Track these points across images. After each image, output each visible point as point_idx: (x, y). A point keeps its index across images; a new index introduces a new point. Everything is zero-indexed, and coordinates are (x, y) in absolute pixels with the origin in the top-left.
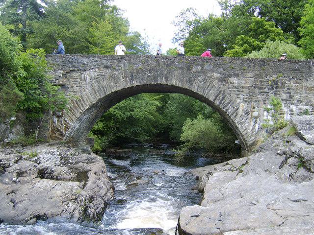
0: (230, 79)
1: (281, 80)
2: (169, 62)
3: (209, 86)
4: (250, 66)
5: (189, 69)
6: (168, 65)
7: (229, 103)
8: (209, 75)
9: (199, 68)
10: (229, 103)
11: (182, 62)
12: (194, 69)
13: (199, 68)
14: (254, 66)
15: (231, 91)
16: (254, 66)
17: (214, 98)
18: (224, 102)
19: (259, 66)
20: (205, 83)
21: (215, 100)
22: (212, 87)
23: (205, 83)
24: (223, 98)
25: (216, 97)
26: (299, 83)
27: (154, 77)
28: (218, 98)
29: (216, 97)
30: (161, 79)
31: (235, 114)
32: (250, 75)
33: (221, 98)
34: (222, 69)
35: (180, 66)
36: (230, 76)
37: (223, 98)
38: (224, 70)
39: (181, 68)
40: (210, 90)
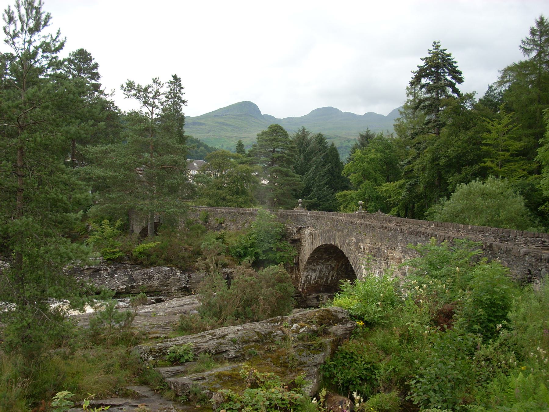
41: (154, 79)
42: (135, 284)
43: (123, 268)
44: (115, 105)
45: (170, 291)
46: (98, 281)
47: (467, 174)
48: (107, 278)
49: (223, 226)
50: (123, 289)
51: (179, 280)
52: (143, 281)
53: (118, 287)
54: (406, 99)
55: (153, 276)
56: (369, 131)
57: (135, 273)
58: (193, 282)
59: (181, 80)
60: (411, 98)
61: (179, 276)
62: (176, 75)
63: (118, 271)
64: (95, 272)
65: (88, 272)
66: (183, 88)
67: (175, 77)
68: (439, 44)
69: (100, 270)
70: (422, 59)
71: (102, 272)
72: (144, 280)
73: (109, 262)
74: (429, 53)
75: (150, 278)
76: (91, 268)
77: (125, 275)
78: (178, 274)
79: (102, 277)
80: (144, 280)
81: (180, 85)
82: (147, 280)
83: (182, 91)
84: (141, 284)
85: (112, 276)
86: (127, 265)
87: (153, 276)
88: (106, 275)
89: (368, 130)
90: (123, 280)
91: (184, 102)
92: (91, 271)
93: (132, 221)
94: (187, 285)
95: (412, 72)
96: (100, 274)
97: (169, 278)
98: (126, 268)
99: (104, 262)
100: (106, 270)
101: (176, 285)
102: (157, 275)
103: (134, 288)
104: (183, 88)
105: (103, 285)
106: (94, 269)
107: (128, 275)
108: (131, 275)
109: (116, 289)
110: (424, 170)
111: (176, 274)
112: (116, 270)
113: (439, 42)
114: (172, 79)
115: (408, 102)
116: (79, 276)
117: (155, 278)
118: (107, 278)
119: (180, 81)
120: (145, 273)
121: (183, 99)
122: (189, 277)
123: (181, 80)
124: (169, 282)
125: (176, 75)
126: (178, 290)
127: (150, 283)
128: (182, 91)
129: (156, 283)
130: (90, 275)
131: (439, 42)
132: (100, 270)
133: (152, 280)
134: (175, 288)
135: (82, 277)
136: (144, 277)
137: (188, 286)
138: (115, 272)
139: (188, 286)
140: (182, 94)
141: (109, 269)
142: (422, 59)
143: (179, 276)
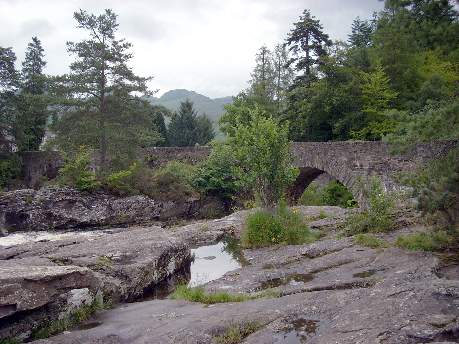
0: (354, 162)
1: (393, 162)
2: (313, 148)
3: (339, 168)
4: (367, 149)
5: (326, 153)
6: (312, 151)
7: (353, 185)
8: (339, 159)
9: (333, 152)
10: (353, 185)
11: (321, 148)
12: (329, 154)
13: (333, 152)
14: (371, 149)
15: (354, 173)
16: (371, 149)
17: (343, 179)
18: (350, 184)
19: (374, 148)
20: (337, 166)
21: (343, 181)
22: (342, 170)
23: (337, 166)
24: (349, 180)
25: (344, 179)
26: (407, 164)
27: (304, 162)
28: (345, 180)
29: (344, 179)
30: (308, 163)
31: (357, 195)
32: (369, 157)
33: (348, 180)
34: (347, 153)
35: (320, 151)
36: (353, 159)
37: (349, 180)
38: (349, 153)
39: (321, 153)
40: (340, 172)
41: (107, 10)
42: (114, 215)
43: (100, 199)
44: (13, 51)
45: (144, 221)
46: (76, 212)
47: (351, 119)
48: (84, 210)
49: (154, 164)
50: (102, 220)
51: (153, 209)
52: (122, 211)
53: (99, 218)
54: (256, 64)
55: (131, 206)
56: (189, 99)
57: (114, 203)
58: (164, 212)
59: (41, 43)
60: (260, 63)
61: (153, 205)
62: (36, 37)
63: (95, 202)
64: (70, 203)
65: (62, 204)
66: (43, 50)
67: (35, 40)
68: (309, 12)
69: (75, 201)
70: (294, 24)
71: (77, 203)
72: (123, 210)
73: (85, 192)
74: (301, 19)
75: (129, 207)
76: (66, 200)
77: (103, 205)
78: (153, 203)
79: (78, 208)
80: (123, 210)
81: (40, 48)
82: (125, 210)
83: (42, 52)
84: (119, 214)
85: (89, 208)
86: (105, 195)
87: (131, 206)
88: (82, 207)
89: (188, 98)
90: (102, 211)
91: (44, 63)
92: (66, 202)
93: (28, 168)
94: (158, 214)
95: (287, 34)
96: (75, 206)
97: (144, 208)
98: (103, 198)
99: (78, 193)
100: (81, 201)
101: (149, 215)
102: (134, 205)
103: (113, 219)
104: (43, 50)
105: (83, 216)
106: (70, 200)
107: (106, 205)
108: (109, 205)
109: (97, 220)
110: (304, 117)
111: (151, 204)
112: (93, 200)
113: (309, 10)
114: (32, 42)
115: (258, 67)
116: (54, 208)
117: (132, 208)
118: (84, 210)
119: (40, 44)
120: (123, 203)
121: (43, 61)
122: (162, 206)
123: (41, 43)
124: (144, 211)
125: (36, 37)
126: (150, 220)
127: (128, 214)
128: (42, 52)
129: (133, 212)
130: (65, 207)
131: (309, 10)
132: (75, 201)
133: (129, 210)
134: (149, 218)
135: (57, 209)
136: (123, 207)
137: (159, 216)
138: (91, 203)
139: (159, 216)
140: (43, 56)
141: (84, 200)
142: (294, 24)
143: (153, 205)
